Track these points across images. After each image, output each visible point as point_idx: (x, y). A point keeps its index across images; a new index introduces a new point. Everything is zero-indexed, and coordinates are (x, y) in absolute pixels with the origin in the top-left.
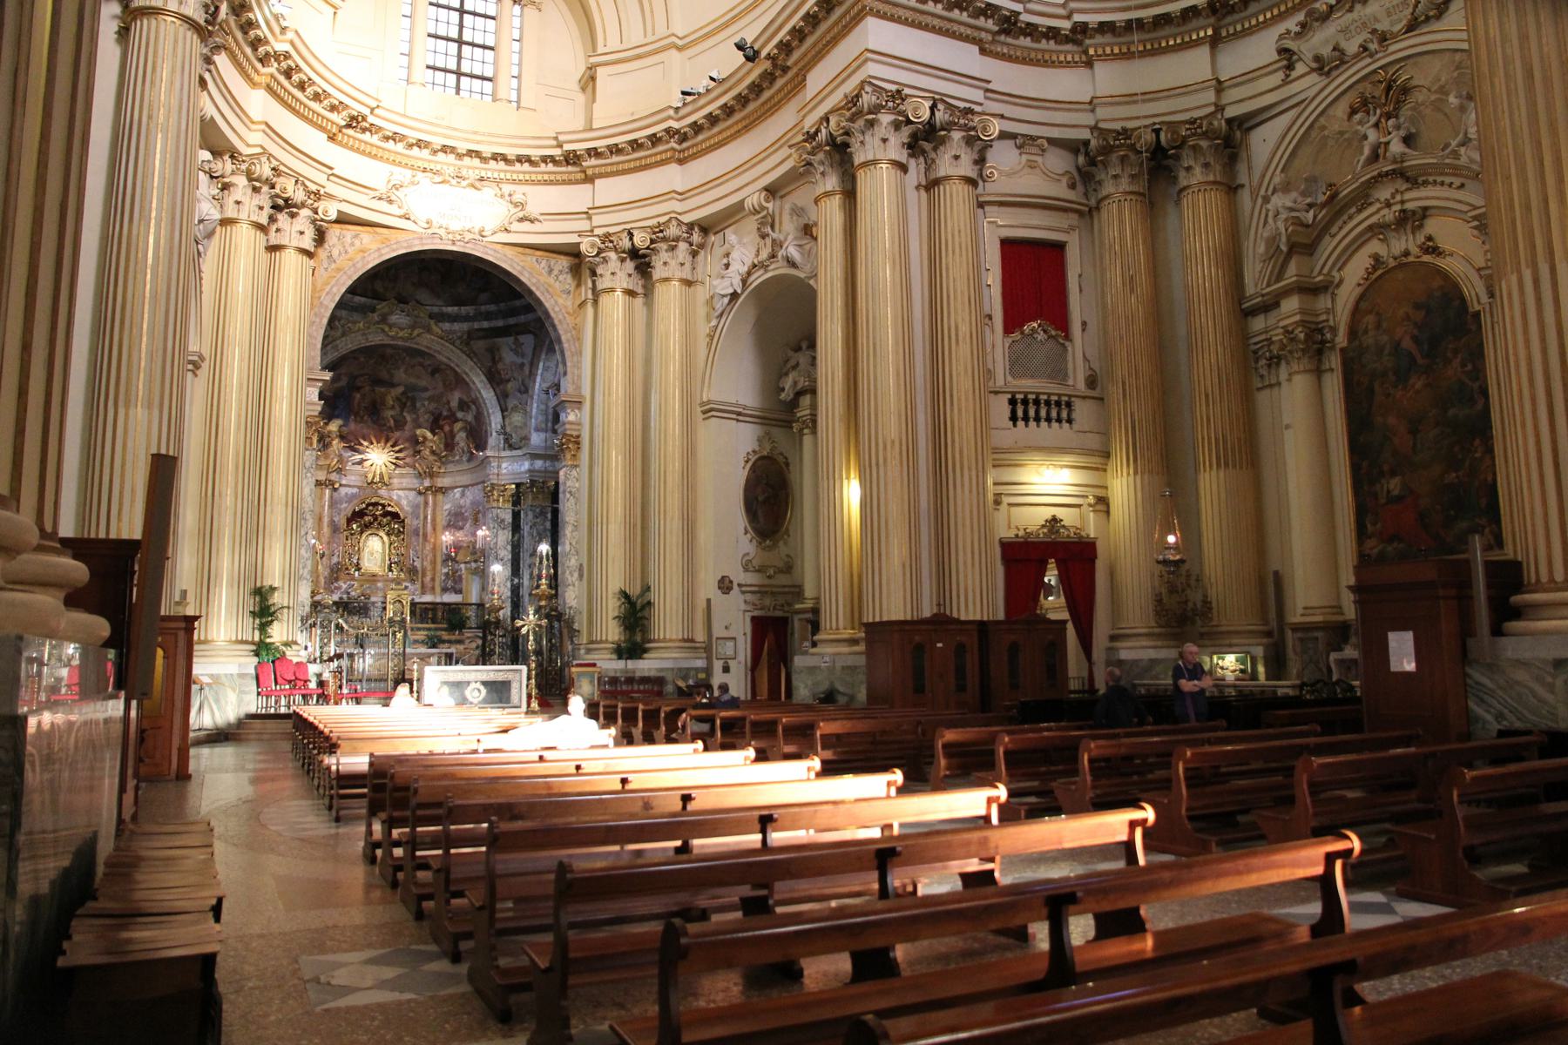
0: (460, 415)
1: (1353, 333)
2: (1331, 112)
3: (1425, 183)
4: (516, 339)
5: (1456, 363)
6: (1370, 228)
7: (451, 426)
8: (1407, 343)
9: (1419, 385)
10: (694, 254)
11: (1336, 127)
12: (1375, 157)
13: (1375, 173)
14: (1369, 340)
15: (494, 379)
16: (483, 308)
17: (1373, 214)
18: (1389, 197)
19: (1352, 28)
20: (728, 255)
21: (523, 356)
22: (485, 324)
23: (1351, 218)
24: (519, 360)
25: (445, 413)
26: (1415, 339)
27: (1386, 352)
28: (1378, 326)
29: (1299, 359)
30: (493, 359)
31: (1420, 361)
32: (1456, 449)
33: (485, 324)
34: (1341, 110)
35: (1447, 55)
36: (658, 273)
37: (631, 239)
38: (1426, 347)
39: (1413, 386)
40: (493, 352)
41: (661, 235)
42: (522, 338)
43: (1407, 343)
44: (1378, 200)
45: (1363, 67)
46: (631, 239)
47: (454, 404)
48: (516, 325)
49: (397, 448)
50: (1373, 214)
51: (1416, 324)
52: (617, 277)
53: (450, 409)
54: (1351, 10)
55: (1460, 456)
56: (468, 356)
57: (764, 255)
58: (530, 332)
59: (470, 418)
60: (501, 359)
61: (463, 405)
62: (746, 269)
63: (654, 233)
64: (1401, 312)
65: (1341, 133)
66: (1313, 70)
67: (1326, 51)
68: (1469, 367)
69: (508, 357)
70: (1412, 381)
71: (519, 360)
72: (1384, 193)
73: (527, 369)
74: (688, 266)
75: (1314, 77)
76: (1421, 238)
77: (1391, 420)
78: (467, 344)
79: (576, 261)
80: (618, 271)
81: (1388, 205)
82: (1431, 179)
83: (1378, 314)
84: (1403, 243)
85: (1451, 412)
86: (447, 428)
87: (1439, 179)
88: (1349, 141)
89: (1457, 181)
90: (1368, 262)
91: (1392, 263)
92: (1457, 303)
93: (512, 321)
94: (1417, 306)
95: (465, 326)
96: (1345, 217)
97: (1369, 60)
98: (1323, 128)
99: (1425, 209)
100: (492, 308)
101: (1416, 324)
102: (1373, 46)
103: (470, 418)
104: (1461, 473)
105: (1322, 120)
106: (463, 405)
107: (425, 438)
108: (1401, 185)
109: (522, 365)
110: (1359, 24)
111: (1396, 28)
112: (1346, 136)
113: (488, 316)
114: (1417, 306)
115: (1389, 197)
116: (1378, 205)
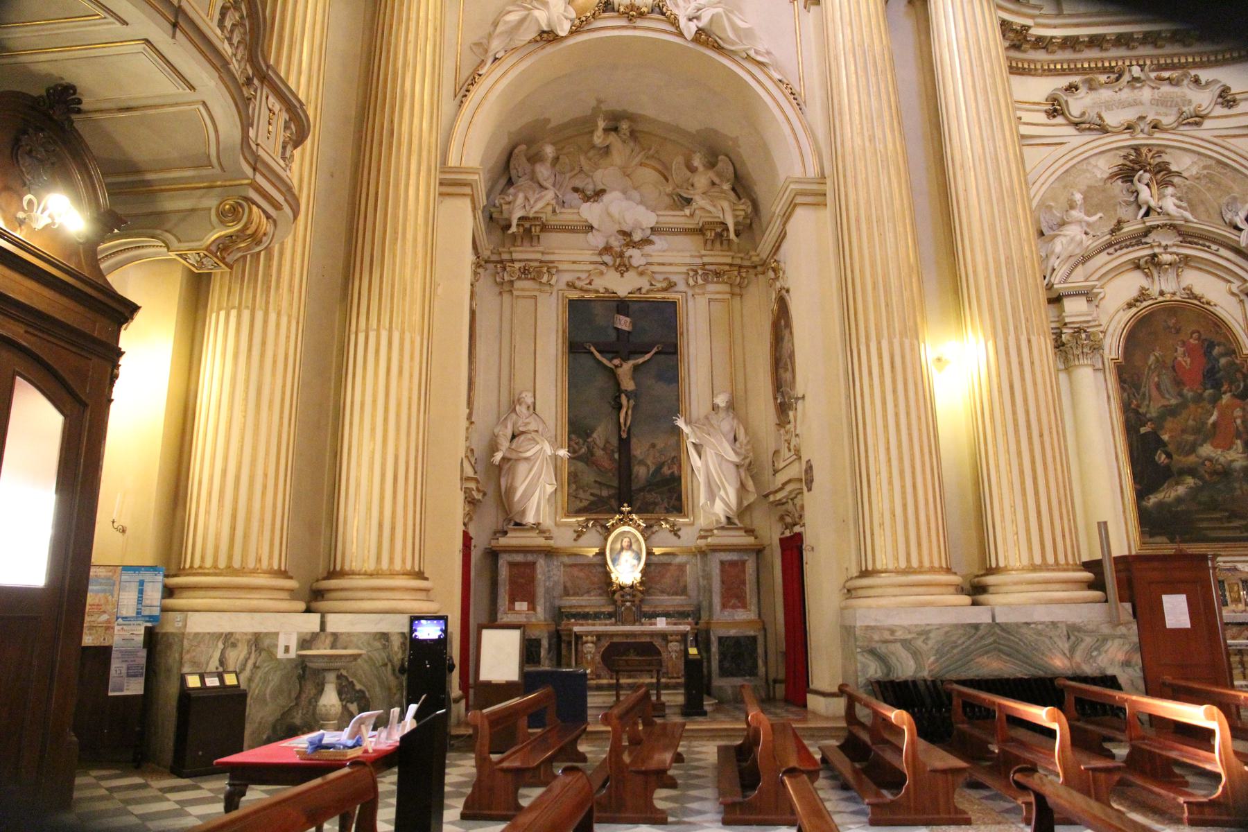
35: (1195, 158)
45: (1125, 140)
75: (1071, 130)
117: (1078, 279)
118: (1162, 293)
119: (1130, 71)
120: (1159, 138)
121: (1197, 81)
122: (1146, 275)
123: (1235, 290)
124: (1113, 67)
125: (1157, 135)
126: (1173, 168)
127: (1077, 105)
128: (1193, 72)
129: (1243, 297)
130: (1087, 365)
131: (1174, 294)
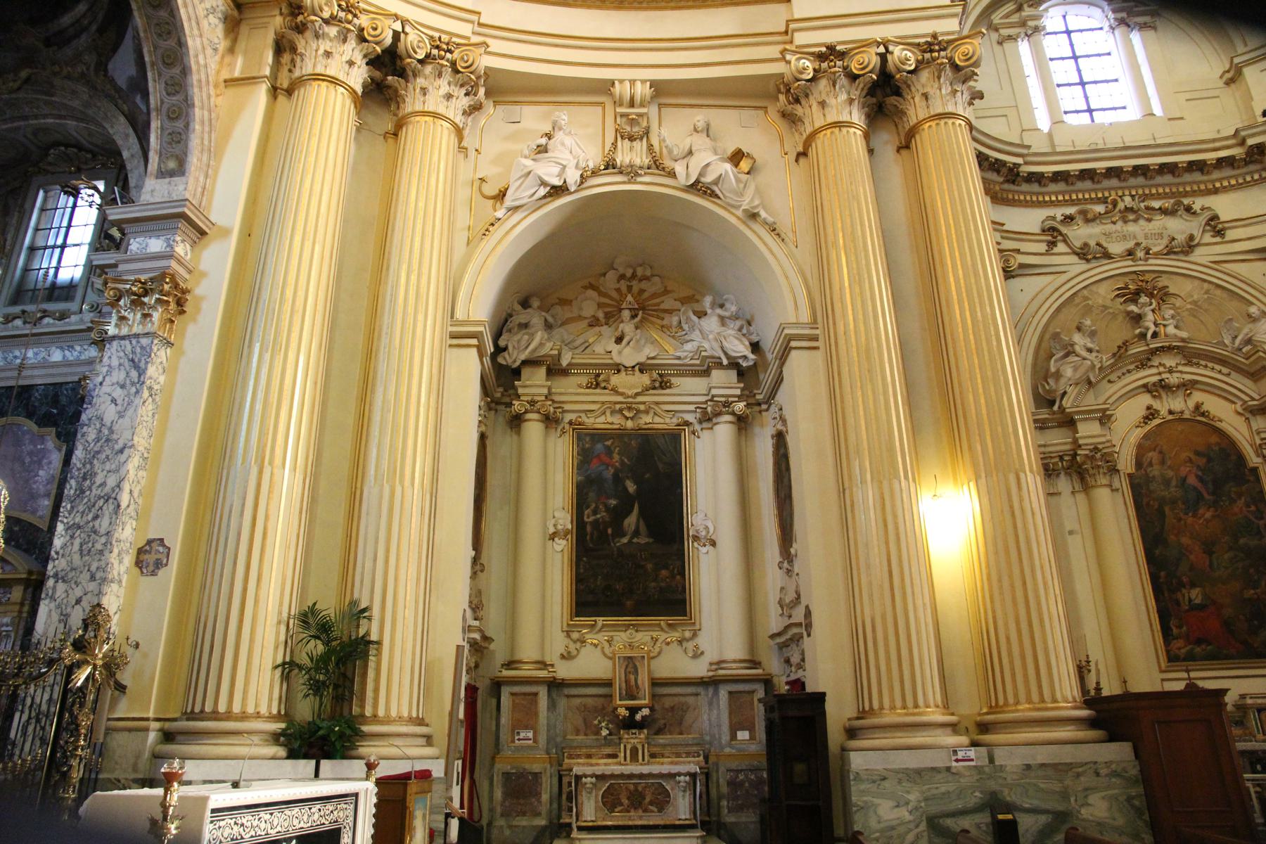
1: (1139, 464)
2: (1094, 288)
3: (1198, 365)
5: (1241, 503)
6: (1145, 386)
8: (1192, 480)
9: (1208, 515)
11: (1100, 301)
12: (1155, 335)
13: (1167, 344)
14: (1155, 471)
17: (1149, 375)
18: (1174, 365)
19: (1114, 235)
23: (1129, 371)
26: (1201, 479)
27: (1174, 483)
28: (1163, 462)
29: (1105, 474)
31: (1207, 497)
32: (1252, 571)
34: (1105, 293)
38: (1210, 486)
39: (1203, 515)
43: (1192, 480)
44: (1164, 365)
45: (1126, 266)
50: (1149, 375)
51: (1198, 467)
54: (1114, 223)
55: (1256, 577)
64: (1184, 455)
65: (1106, 307)
66: (1077, 254)
67: (1092, 243)
68: (1253, 508)
70: (1201, 511)
72: (1170, 361)
75: (1074, 259)
76: (1191, 404)
77: (1185, 540)
81: (1171, 371)
82: (1203, 363)
83: (1160, 452)
84: (1177, 403)
85: (1242, 541)
87: (1210, 365)
88: (1114, 316)
89: (1225, 370)
90: (1143, 412)
91: (1171, 417)
92: (1234, 458)
94: (1197, 453)
96: (1124, 370)
97: (1130, 263)
98: (1086, 298)
99: (1197, 382)
101: (1198, 467)
102: (1140, 254)
104: (1258, 591)
105: (1085, 292)
108: (1178, 359)
110: (1120, 235)
111: (1155, 249)
112: (1111, 311)
114: (1197, 453)
115: (1174, 365)
116: (1161, 369)
117: (1091, 401)
118: (1171, 412)
119: (1123, 200)
120: (1155, 264)
121: (1188, 209)
122: (1154, 397)
123: (1240, 410)
124: (1107, 198)
125: (1151, 261)
126: (1171, 290)
127: (1080, 233)
128: (1186, 201)
129: (1248, 415)
130: (1102, 486)
131: (1182, 412)
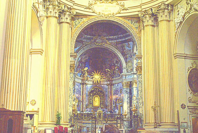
0: (116, 65)
4: (128, 43)
7: (114, 68)
10: (170, 13)
15: (124, 54)
16: (119, 36)
20: (178, 11)
21: (130, 48)
22: (120, 40)
24: (129, 49)
25: (113, 64)
30: (123, 49)
33: (120, 40)
36: (160, 19)
37: (152, 11)
40: (123, 47)
41: (160, 8)
42: (129, 43)
46: (152, 11)
47: (115, 62)
48: (128, 39)
49: (101, 74)
52: (149, 22)
53: (114, 63)
56: (117, 49)
57: (188, 9)
58: (131, 41)
59: (119, 65)
60: (125, 49)
61: (117, 62)
62: (184, 14)
63: (158, 8)
69: (127, 48)
71: (129, 49)
73: (131, 51)
74: (168, 16)
78: (116, 46)
79: (137, 19)
80: (149, 20)
86: (113, 68)
93: (127, 39)
95: (115, 41)
100: (122, 36)
103: (119, 65)
106: (117, 62)
107: (108, 71)
109: (130, 50)
113: (121, 38)
